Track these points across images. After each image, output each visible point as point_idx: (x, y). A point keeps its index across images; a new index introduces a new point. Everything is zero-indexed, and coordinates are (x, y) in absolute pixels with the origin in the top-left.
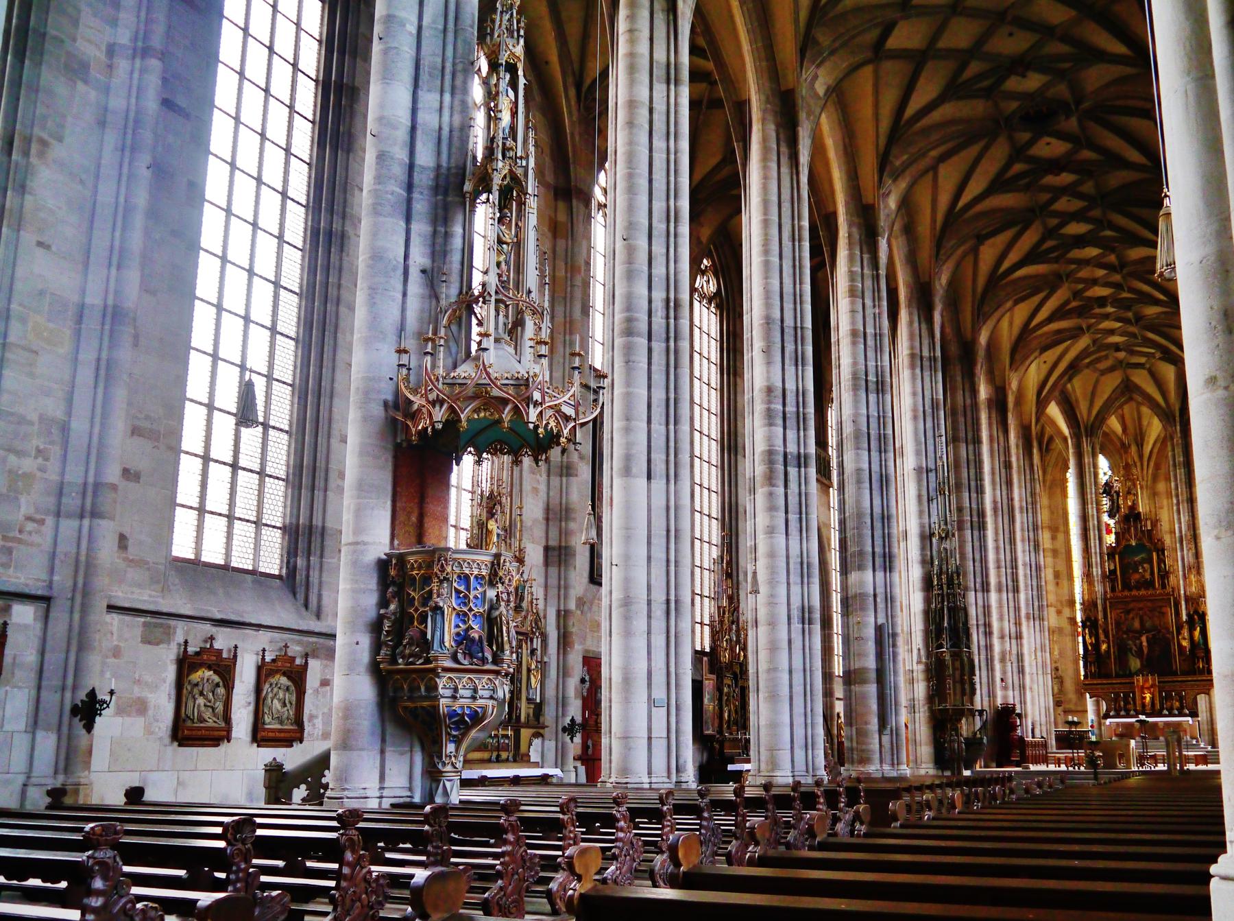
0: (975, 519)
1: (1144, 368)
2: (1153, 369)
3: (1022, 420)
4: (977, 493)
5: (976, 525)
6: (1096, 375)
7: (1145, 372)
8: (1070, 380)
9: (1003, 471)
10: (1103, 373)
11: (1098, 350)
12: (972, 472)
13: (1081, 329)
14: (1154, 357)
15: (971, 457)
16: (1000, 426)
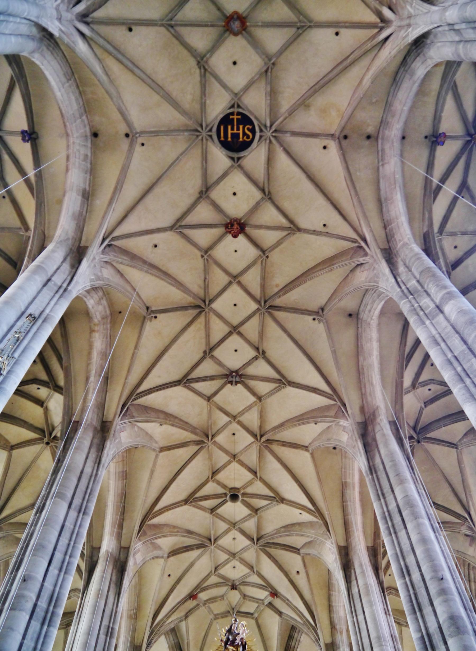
0: (43, 604)
1: (253, 618)
2: (260, 621)
3: (133, 638)
4: (60, 570)
5: (40, 613)
6: (212, 616)
7: (253, 622)
8: (186, 616)
9: (102, 637)
10: (216, 617)
11: (217, 585)
13: (210, 540)
14: (263, 604)
15: (69, 525)
16: (113, 586)
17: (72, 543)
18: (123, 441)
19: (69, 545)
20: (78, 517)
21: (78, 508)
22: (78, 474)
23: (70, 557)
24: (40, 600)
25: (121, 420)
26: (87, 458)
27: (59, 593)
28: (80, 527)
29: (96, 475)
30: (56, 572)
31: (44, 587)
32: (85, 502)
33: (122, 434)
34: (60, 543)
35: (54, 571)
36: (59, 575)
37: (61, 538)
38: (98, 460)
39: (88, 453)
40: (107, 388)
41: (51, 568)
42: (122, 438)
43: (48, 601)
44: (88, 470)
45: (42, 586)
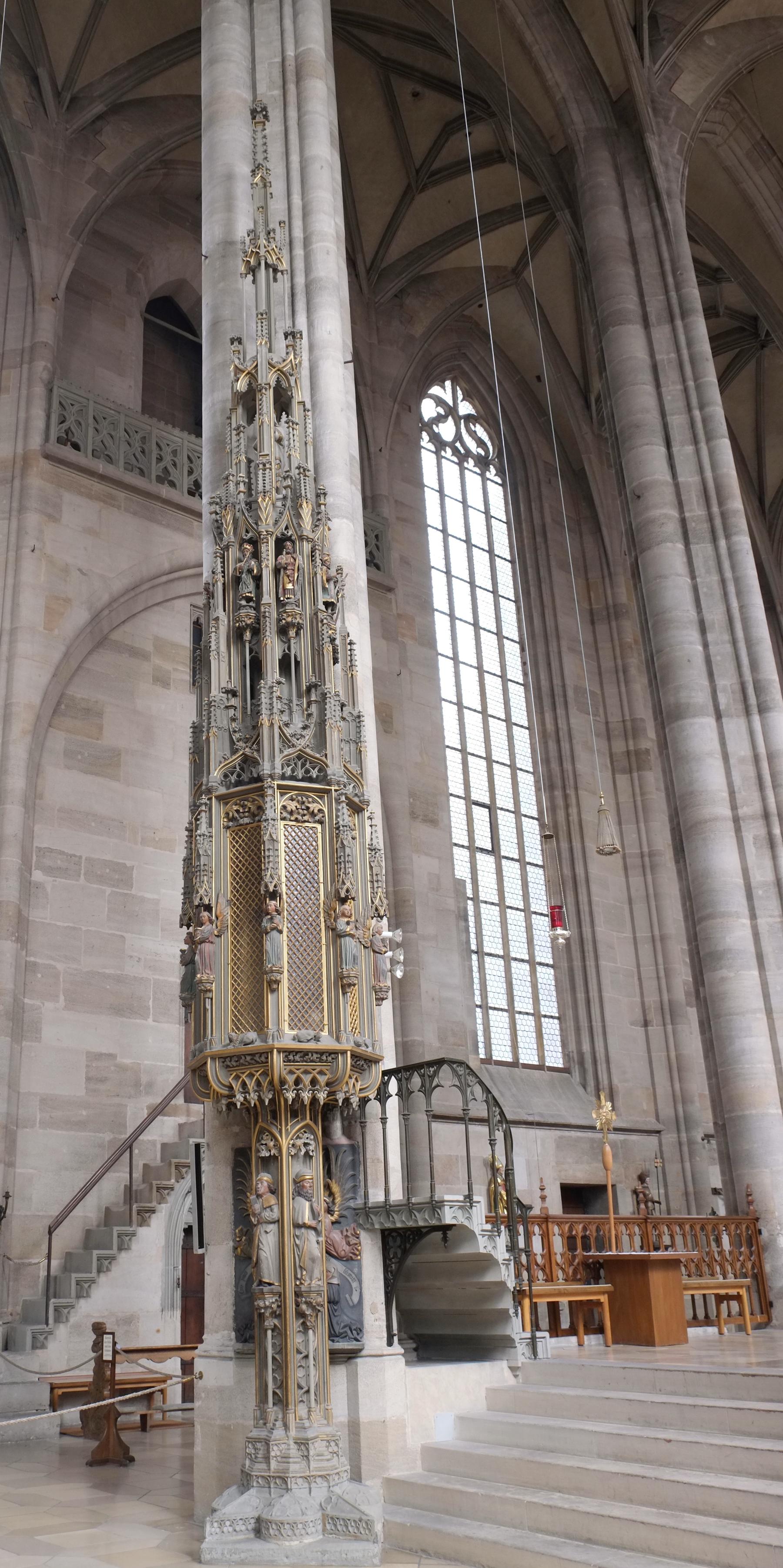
4: (696, 441)
12: (672, 390)
15: (665, 355)
17: (691, 383)
18: (689, 101)
19: (686, 390)
20: (674, 330)
21: (665, 314)
22: (626, 252)
23: (702, 407)
24: (686, 508)
25: (654, 61)
26: (625, 207)
27: (715, 479)
28: (689, 345)
29: (665, 224)
30: (690, 449)
31: (681, 486)
32: (673, 294)
33: (677, 88)
34: (667, 398)
35: (684, 451)
36: (698, 451)
37: (664, 390)
38: (651, 193)
39: (623, 195)
40: (574, 26)
41: (675, 449)
42: (681, 97)
43: (702, 501)
44: (642, 227)
45: (677, 486)
